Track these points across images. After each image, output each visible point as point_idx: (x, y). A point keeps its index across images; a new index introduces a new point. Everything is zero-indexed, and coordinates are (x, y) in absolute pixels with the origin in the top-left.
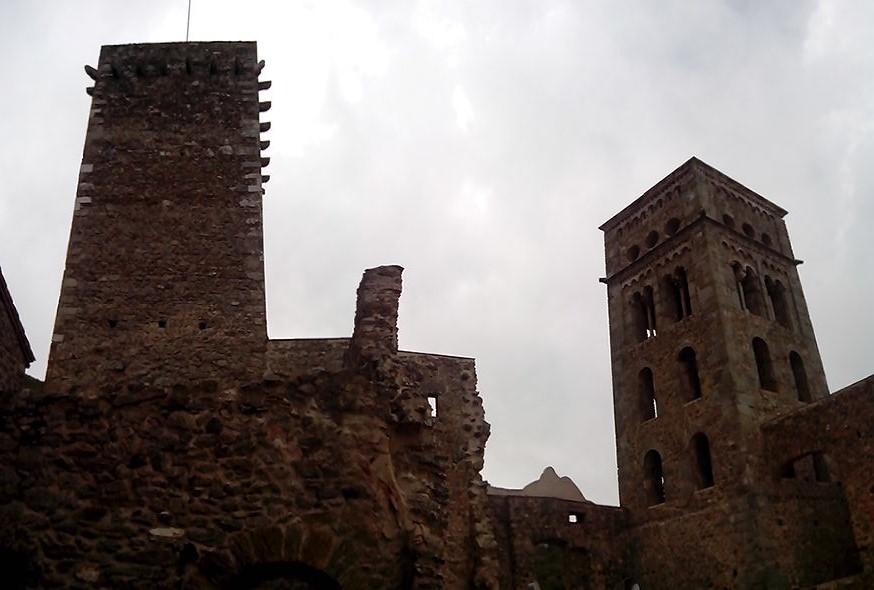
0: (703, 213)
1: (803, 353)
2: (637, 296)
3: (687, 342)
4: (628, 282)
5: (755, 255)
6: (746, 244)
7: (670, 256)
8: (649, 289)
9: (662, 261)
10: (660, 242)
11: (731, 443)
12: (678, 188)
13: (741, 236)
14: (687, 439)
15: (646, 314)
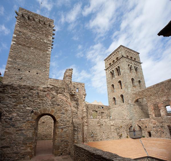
0: (123, 56)
1: (141, 80)
2: (111, 72)
3: (120, 80)
4: (109, 70)
5: (132, 63)
6: (131, 61)
7: (117, 64)
8: (113, 71)
9: (115, 65)
10: (115, 62)
11: (127, 96)
12: (118, 51)
13: (130, 59)
14: (119, 95)
15: (112, 75)
